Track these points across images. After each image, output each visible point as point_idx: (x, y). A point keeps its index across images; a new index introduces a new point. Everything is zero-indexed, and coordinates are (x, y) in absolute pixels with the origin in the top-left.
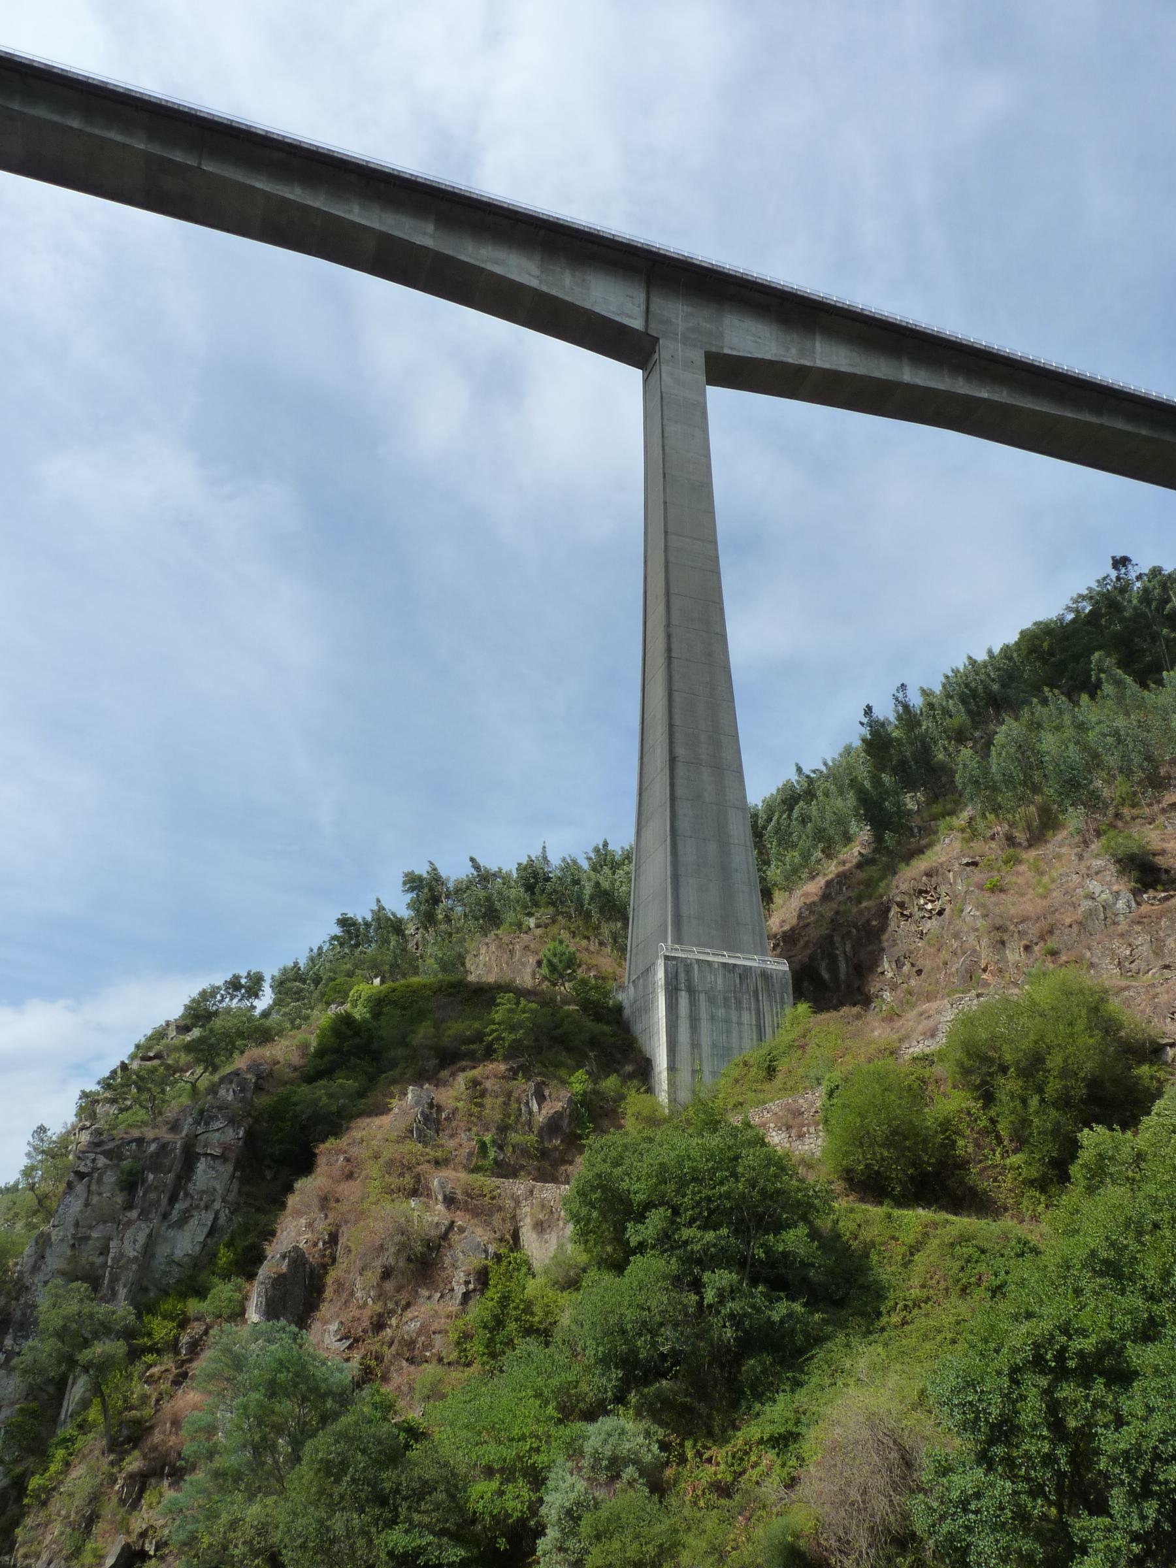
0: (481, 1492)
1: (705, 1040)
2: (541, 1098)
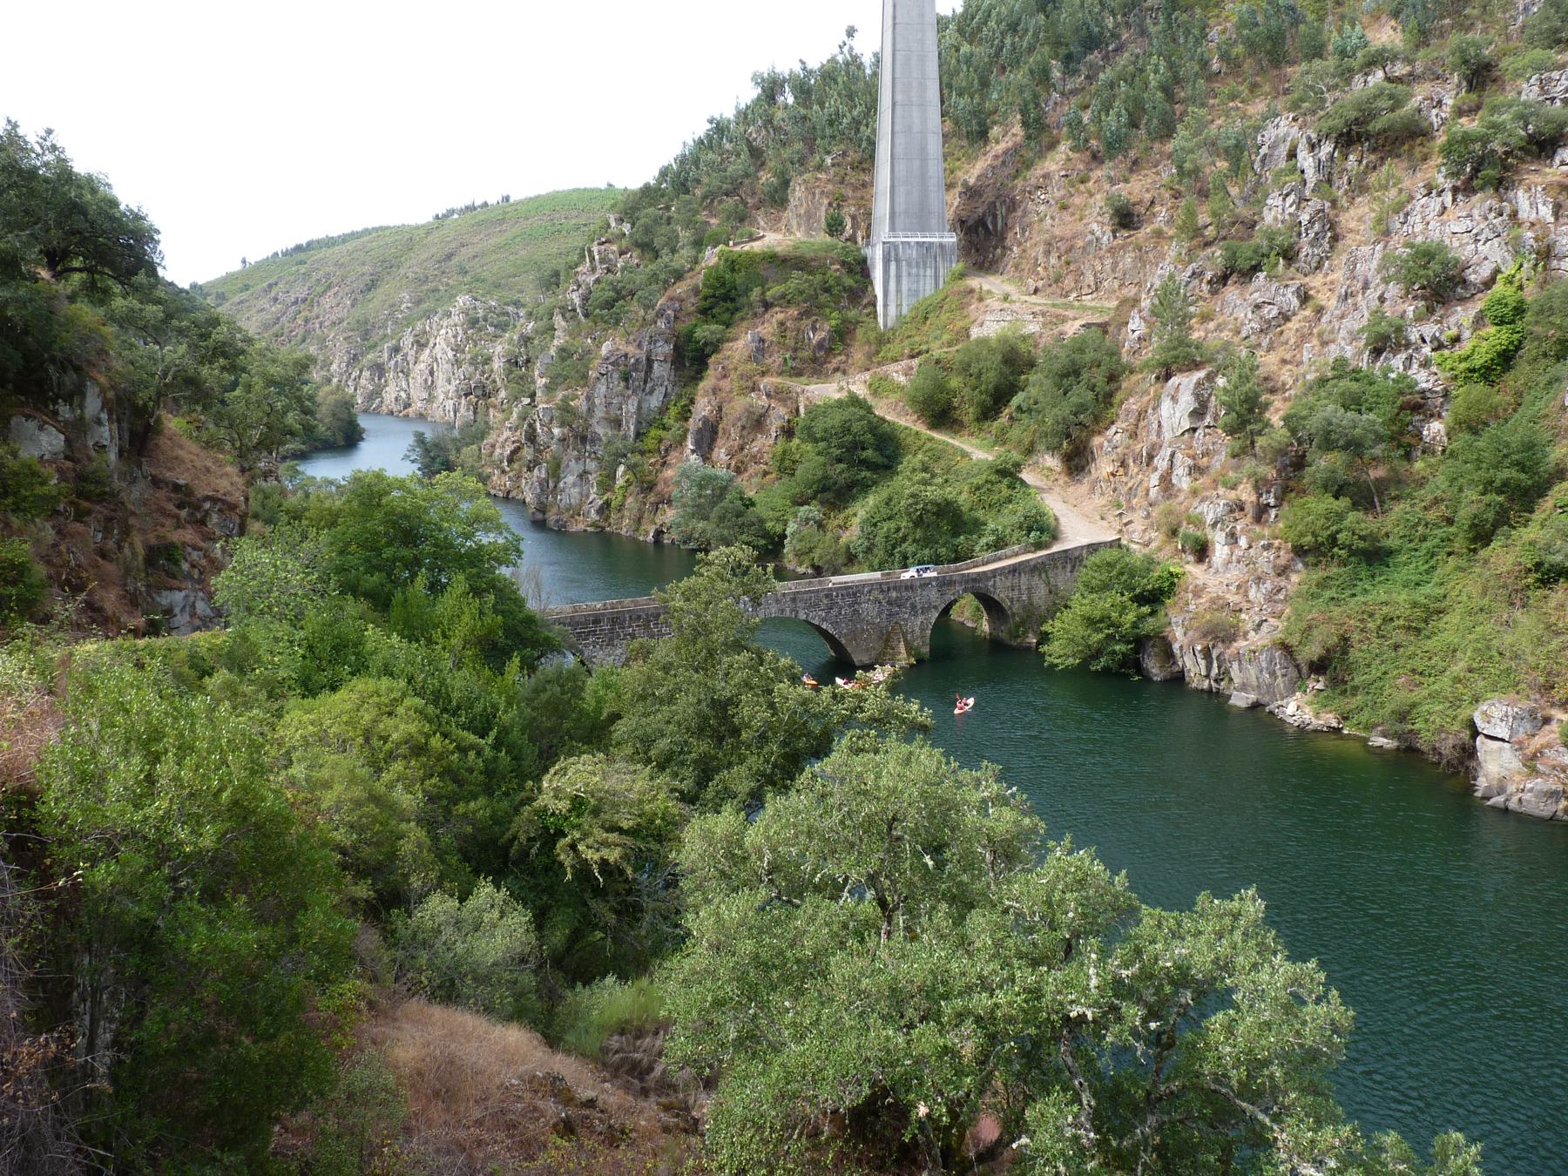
0: (769, 525)
1: (905, 288)
2: (814, 329)
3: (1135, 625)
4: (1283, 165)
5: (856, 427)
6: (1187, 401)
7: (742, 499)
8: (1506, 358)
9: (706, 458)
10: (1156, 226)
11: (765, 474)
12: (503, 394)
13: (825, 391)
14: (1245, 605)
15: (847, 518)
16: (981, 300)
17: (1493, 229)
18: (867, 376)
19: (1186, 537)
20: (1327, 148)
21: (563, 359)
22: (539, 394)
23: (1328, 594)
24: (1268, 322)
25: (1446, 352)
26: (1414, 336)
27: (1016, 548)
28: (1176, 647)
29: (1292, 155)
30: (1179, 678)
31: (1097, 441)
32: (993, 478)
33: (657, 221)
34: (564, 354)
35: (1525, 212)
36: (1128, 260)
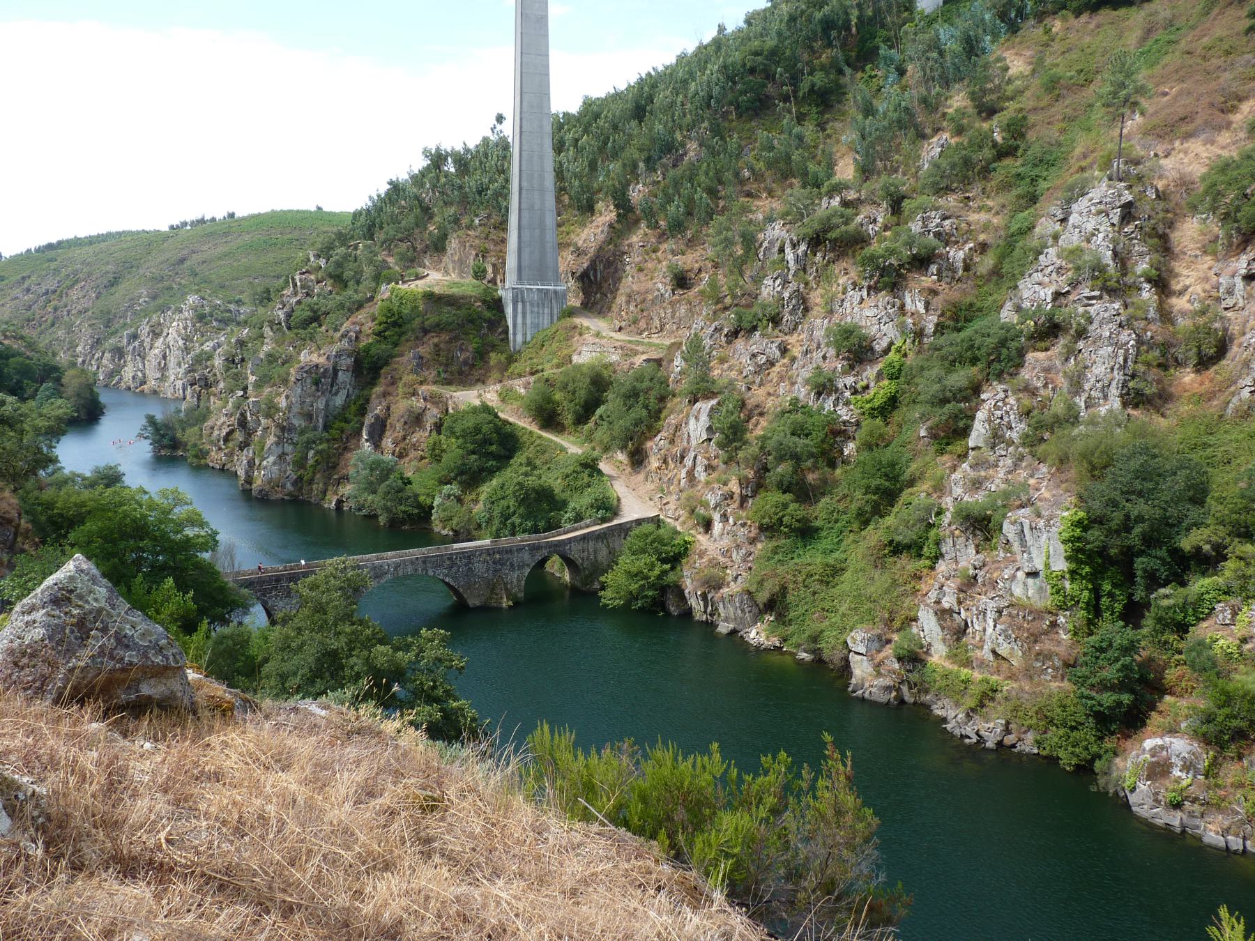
0: (421, 498)
1: (528, 321)
2: (461, 350)
3: (659, 577)
4: (776, 256)
5: (485, 429)
6: (704, 420)
7: (402, 478)
8: (893, 402)
9: (377, 446)
10: (701, 287)
11: (422, 458)
12: (222, 385)
13: (466, 398)
14: (729, 564)
15: (478, 494)
16: (581, 334)
17: (889, 315)
18: (498, 387)
19: (698, 515)
20: (803, 247)
21: (270, 362)
22: (250, 388)
23: (779, 557)
24: (761, 366)
25: (859, 397)
26: (840, 385)
27: (588, 521)
28: (686, 592)
29: (782, 250)
30: (689, 613)
31: (649, 444)
32: (579, 469)
33: (346, 257)
34: (271, 358)
35: (909, 306)
36: (682, 310)
